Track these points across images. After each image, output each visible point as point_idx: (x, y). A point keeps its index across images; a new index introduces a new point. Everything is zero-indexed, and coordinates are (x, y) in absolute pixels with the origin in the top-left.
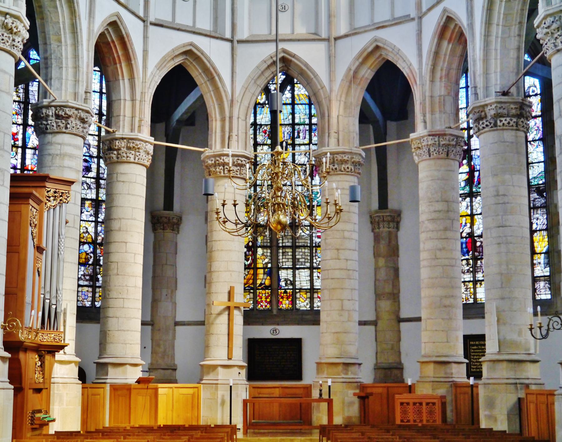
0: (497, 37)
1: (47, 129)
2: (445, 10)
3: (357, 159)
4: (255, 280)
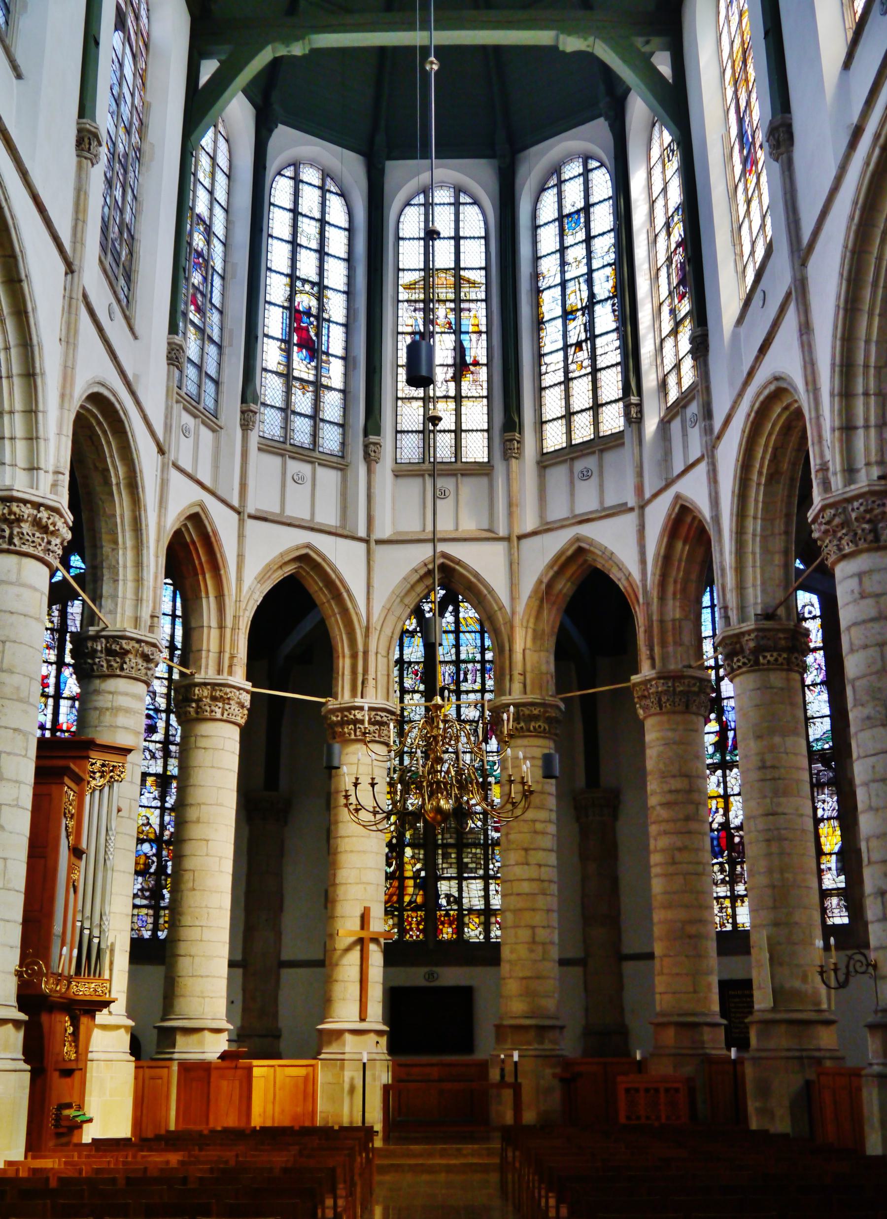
0: (754, 535)
1: (93, 670)
2: (678, 497)
3: (552, 713)
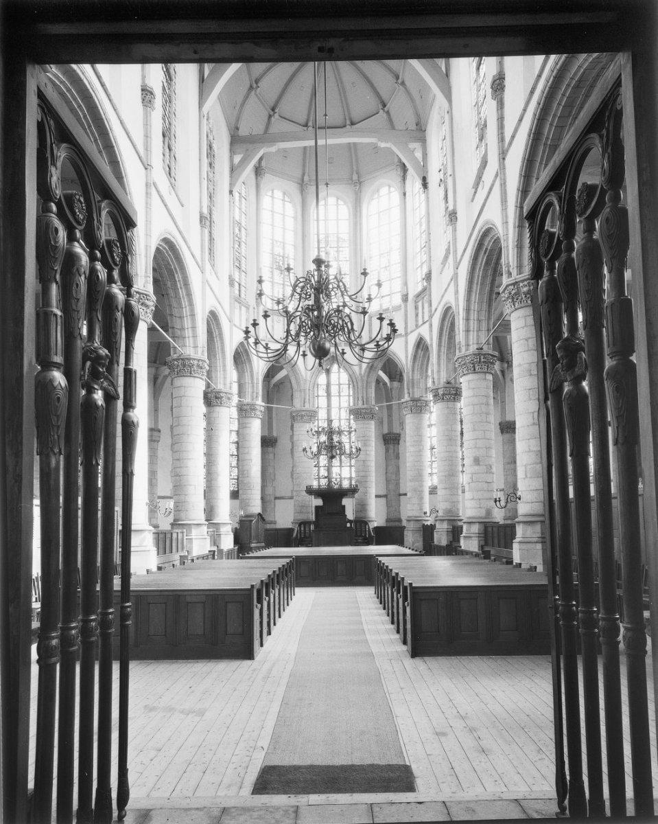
2: (419, 334)
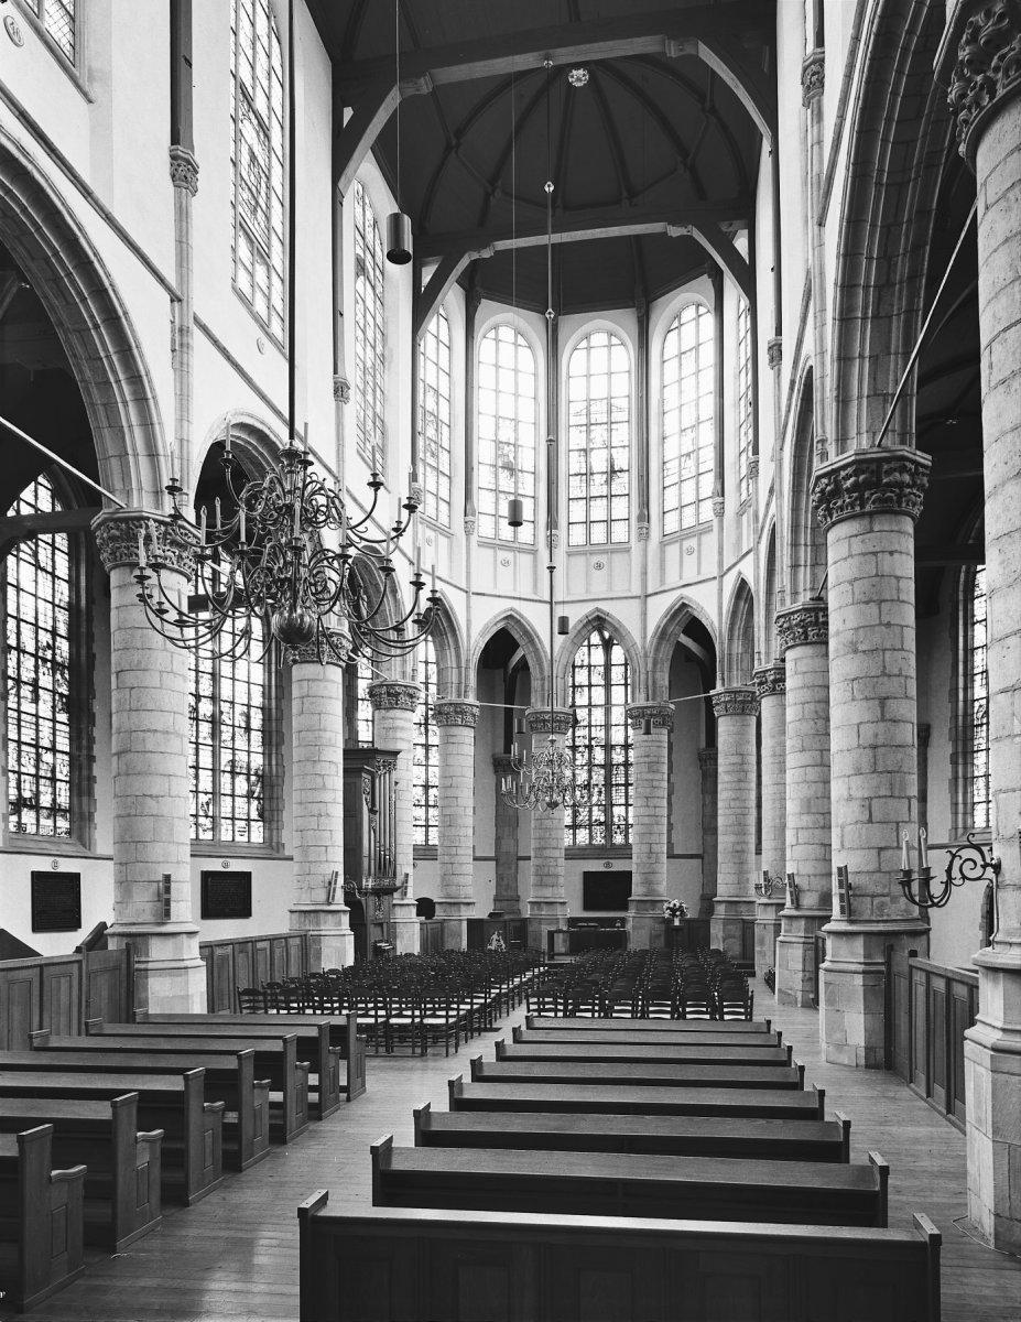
2: (740, 573)
4: (590, 816)
